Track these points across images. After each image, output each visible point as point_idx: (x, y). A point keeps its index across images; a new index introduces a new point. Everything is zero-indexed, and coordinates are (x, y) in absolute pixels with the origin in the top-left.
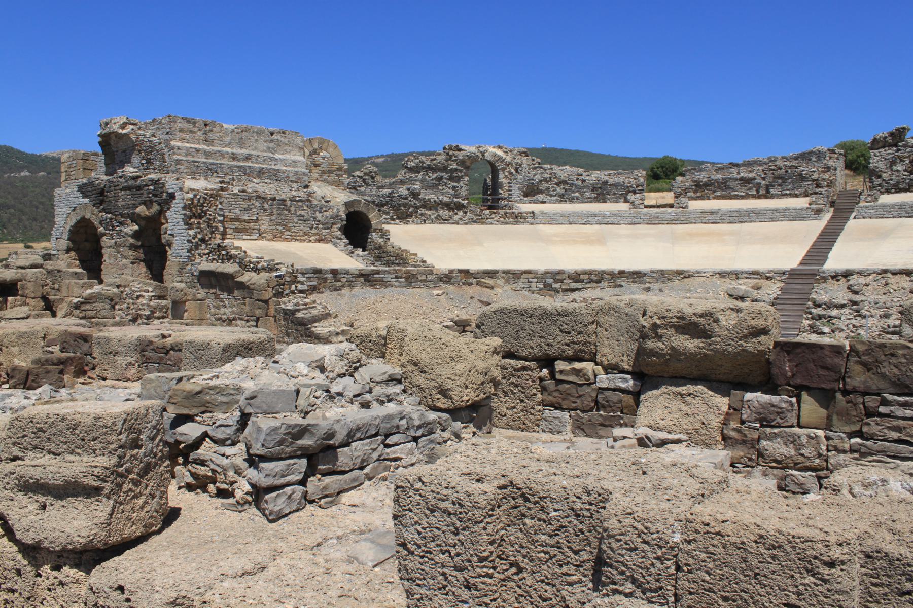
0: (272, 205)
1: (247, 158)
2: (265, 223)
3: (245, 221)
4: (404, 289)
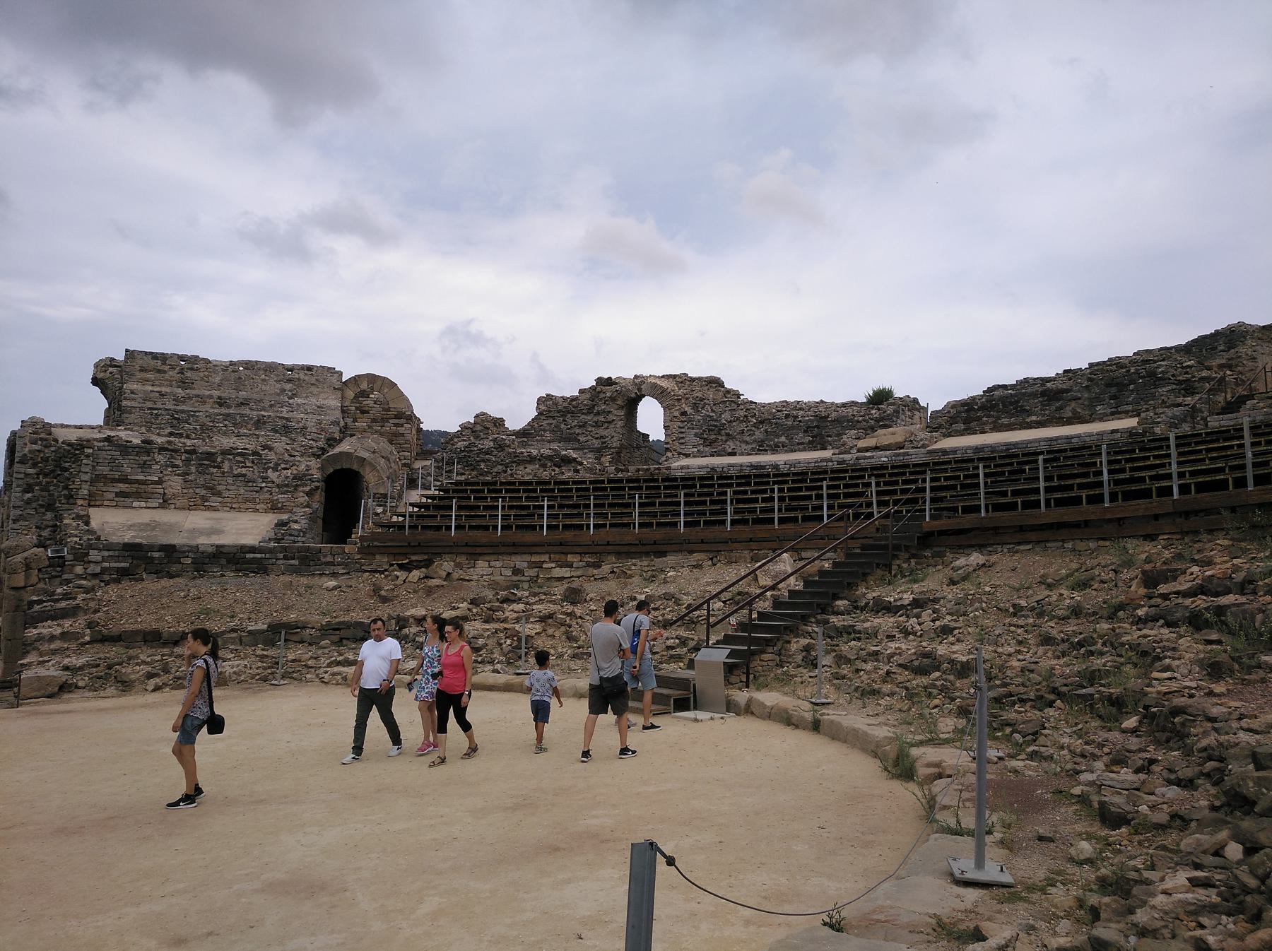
0: (188, 460)
1: (244, 403)
2: (175, 484)
3: (138, 482)
4: (294, 579)
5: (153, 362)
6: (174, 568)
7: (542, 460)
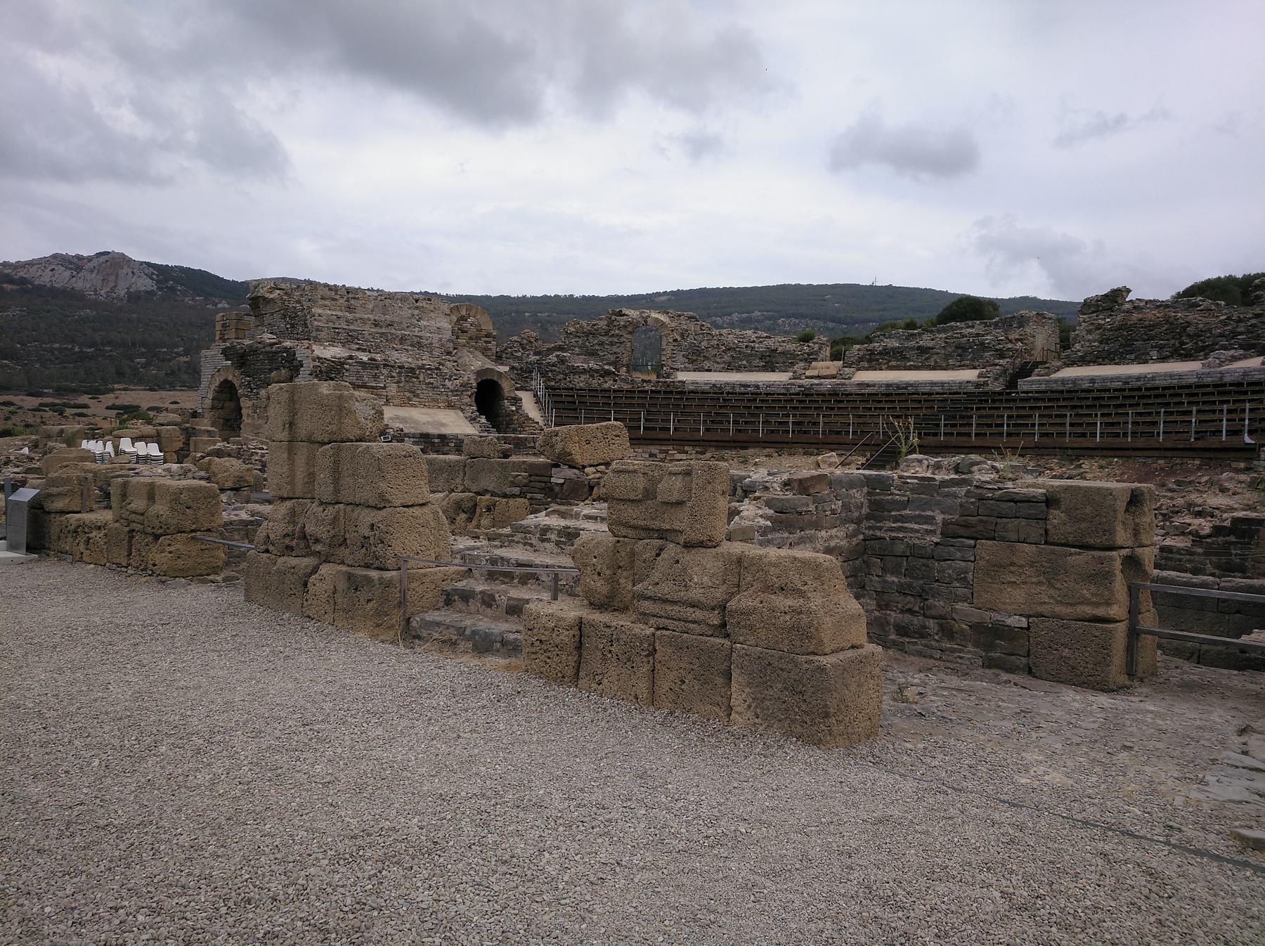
2: (393, 389)
5: (329, 293)
6: (446, 449)
7: (590, 372)
